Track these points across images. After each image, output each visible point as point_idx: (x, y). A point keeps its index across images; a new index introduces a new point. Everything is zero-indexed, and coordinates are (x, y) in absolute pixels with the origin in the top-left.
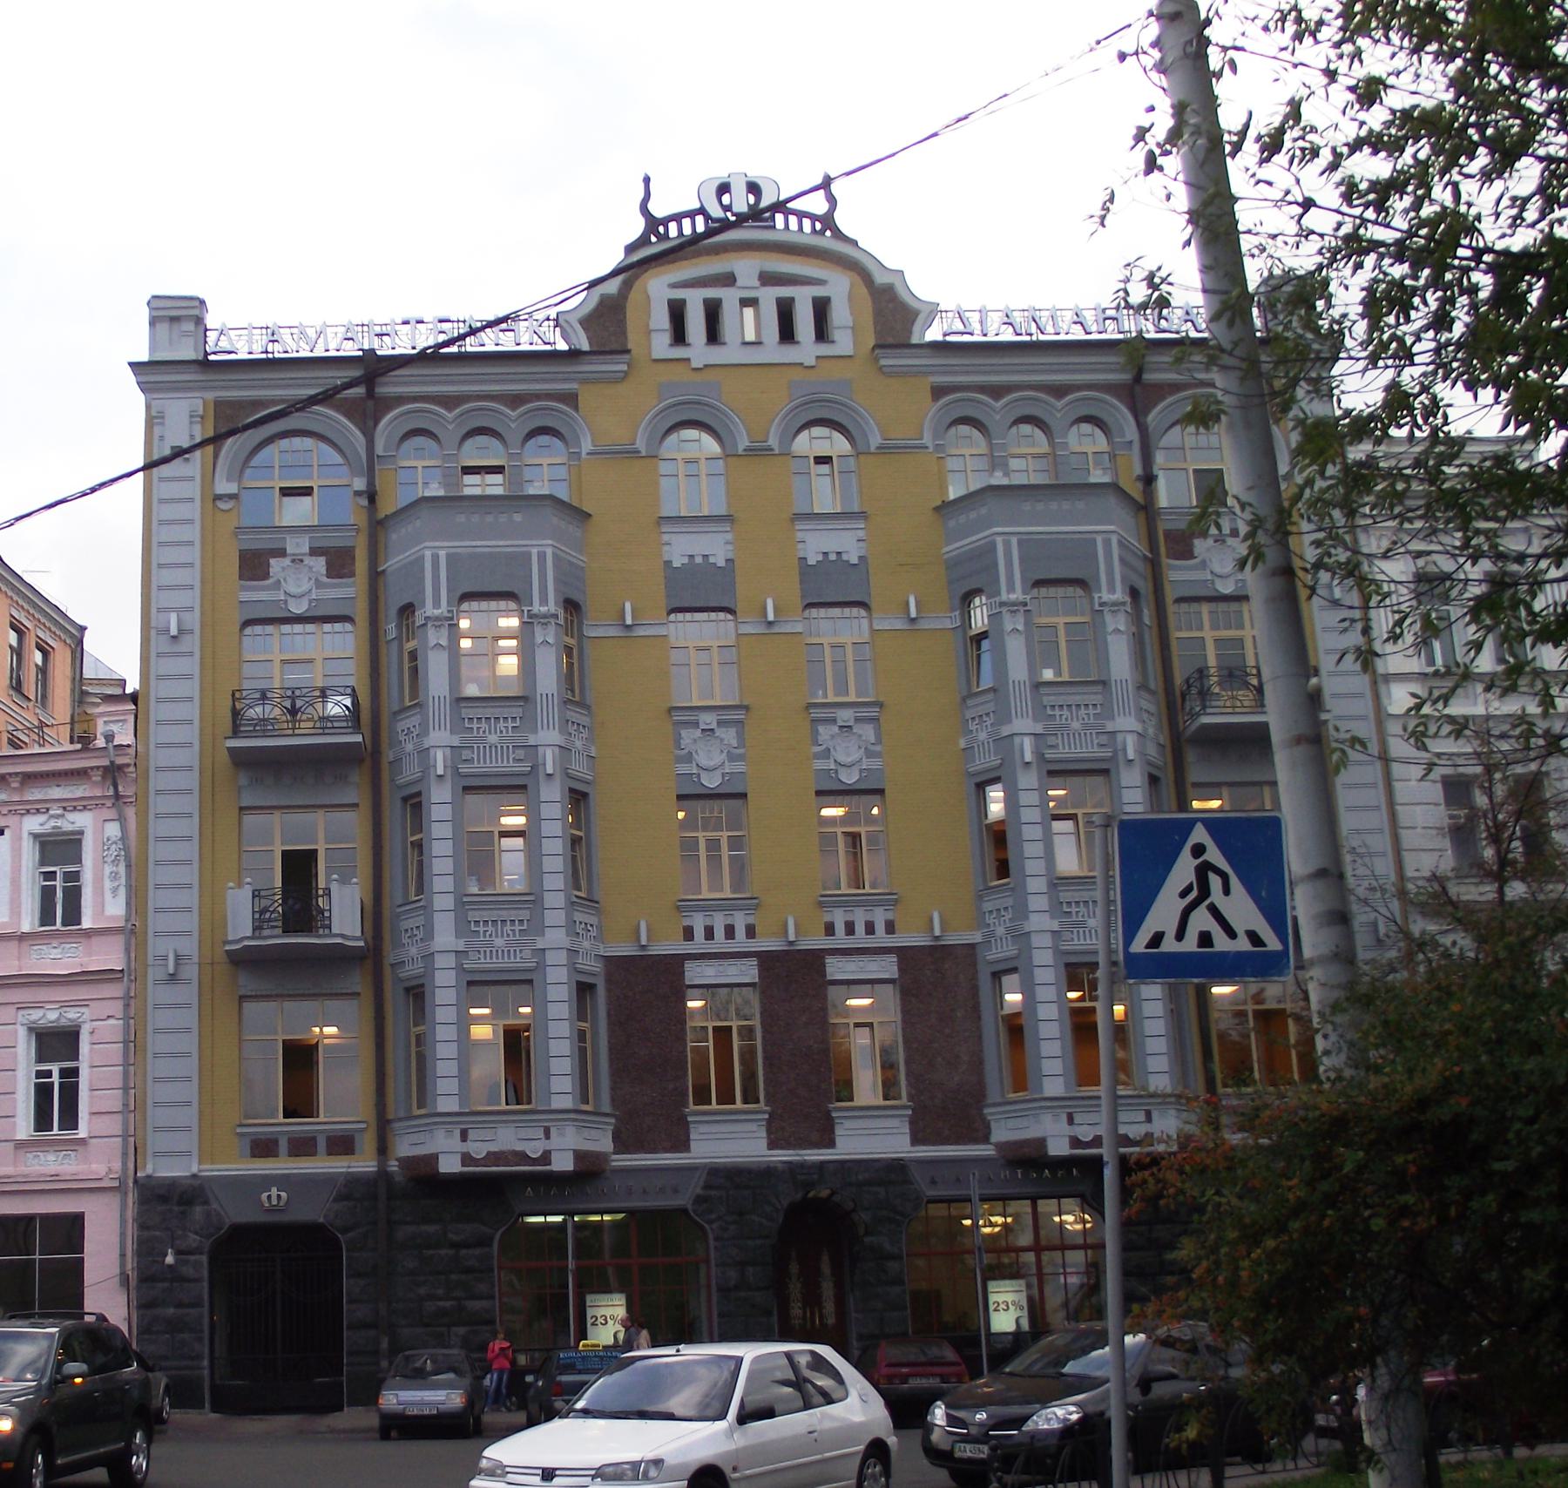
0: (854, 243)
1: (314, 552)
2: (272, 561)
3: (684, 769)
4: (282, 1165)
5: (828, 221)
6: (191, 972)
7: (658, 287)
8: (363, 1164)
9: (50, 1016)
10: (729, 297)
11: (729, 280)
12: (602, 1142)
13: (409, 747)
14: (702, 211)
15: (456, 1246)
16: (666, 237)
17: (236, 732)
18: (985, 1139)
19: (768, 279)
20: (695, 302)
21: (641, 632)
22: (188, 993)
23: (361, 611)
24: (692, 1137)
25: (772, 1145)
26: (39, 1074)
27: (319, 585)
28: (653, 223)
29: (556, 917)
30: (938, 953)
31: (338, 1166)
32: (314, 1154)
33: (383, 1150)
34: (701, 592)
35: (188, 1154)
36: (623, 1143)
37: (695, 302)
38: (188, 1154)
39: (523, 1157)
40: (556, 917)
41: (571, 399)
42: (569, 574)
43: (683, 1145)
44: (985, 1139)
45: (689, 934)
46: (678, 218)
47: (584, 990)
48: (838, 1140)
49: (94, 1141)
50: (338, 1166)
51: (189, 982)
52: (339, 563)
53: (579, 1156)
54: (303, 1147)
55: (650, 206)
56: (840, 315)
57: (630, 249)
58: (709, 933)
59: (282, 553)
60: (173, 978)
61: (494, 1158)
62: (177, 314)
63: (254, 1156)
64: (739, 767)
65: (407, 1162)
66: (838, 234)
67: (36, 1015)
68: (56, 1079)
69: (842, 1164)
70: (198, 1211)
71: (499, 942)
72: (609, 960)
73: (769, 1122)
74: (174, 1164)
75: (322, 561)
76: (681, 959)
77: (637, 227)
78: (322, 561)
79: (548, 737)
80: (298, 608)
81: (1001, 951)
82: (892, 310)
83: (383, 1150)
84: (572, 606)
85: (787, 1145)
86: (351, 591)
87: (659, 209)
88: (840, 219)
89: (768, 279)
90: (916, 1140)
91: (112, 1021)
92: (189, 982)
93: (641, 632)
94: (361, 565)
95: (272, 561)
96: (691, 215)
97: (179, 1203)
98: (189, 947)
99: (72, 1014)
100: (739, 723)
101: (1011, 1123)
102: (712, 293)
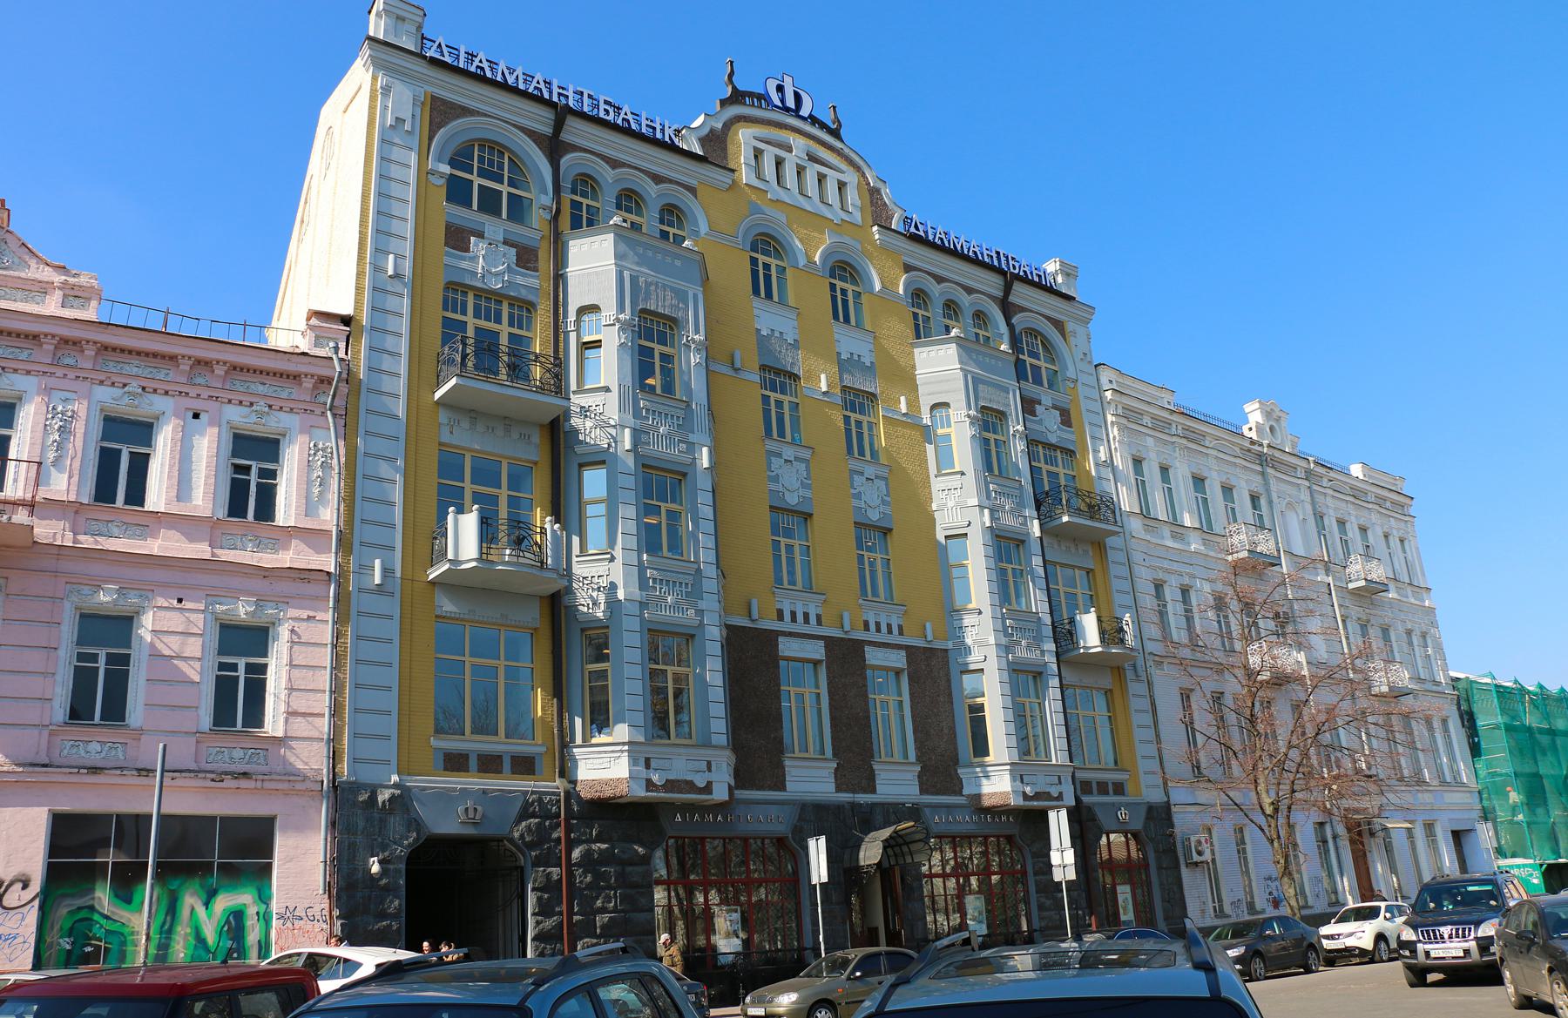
4: (473, 782)
25: (838, 789)
30: (930, 652)
32: (500, 772)
35: (388, 762)
37: (770, 153)
38: (388, 762)
39: (690, 786)
54: (490, 764)
61: (671, 785)
63: (446, 769)
69: (883, 804)
76: (776, 634)
85: (846, 791)
90: (923, 791)
92: (392, 594)
94: (545, 263)
96: (760, 97)
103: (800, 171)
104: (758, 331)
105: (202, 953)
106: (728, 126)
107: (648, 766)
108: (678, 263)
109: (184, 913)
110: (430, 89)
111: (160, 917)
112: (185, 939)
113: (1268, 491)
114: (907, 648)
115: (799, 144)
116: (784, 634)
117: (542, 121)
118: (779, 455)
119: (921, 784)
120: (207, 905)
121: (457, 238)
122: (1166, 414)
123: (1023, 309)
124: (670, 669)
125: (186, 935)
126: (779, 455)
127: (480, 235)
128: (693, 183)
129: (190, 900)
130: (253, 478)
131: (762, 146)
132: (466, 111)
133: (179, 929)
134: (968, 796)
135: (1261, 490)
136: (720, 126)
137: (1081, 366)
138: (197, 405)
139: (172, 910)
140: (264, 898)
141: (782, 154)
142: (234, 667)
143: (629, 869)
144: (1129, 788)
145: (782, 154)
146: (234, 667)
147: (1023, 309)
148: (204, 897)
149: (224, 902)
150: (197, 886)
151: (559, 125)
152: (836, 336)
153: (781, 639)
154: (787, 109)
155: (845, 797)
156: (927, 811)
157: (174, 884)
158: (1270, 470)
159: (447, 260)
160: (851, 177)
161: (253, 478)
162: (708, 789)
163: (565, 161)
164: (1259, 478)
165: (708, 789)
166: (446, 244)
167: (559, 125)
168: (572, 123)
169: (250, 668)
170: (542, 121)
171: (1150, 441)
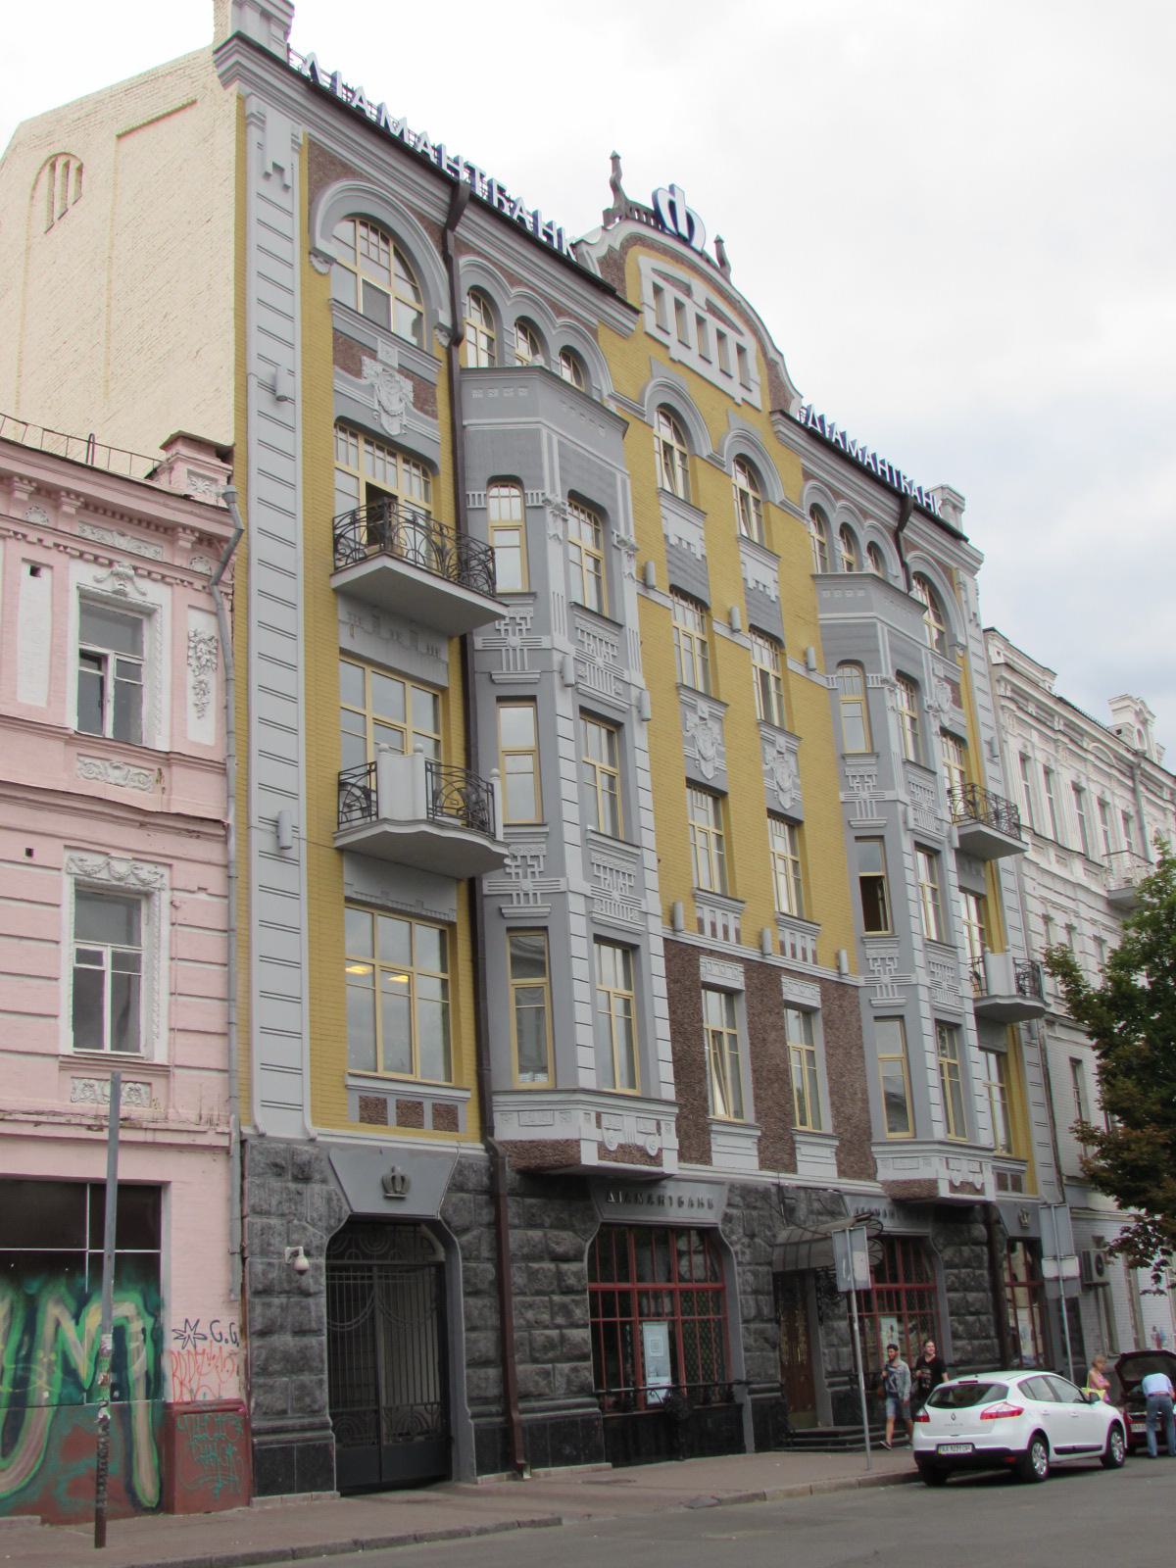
9: (119, 870)
15: (558, 1258)
18: (872, 1177)
22: (294, 878)
24: (714, 1148)
26: (82, 956)
32: (420, 1125)
33: (486, 1128)
44: (872, 1177)
48: (714, 1156)
49: (178, 1071)
51: (296, 862)
55: (624, 184)
63: (362, 1120)
67: (94, 861)
68: (107, 966)
70: (315, 1191)
73: (760, 1139)
81: (888, 998)
83: (486, 1128)
90: (842, 1173)
91: (202, 896)
92: (296, 862)
97: (296, 1179)
99: (146, 872)
101: (899, 1163)
103: (700, 321)
104: (666, 537)
105: (72, 1390)
107: (599, 1125)
109: (46, 1329)
111: (15, 1337)
112: (50, 1372)
113: (1139, 812)
114: (821, 980)
116: (711, 953)
119: (839, 1164)
120: (77, 1317)
122: (1050, 703)
123: (915, 547)
125: (51, 1364)
127: (373, 354)
129: (53, 1310)
130: (111, 672)
133: (40, 1354)
134: (884, 1183)
135: (1131, 811)
136: (617, 246)
137: (971, 629)
138: (39, 555)
139: (30, 1327)
140: (154, 1307)
141: (683, 298)
142: (96, 958)
143: (565, 1267)
144: (1026, 1182)
145: (683, 298)
146: (96, 958)
147: (915, 547)
148: (72, 1303)
149: (93, 1316)
150: (63, 1289)
152: (743, 557)
153: (703, 959)
154: (679, 237)
156: (847, 1199)
157: (33, 1287)
158: (1141, 788)
161: (111, 672)
164: (1128, 796)
166: (335, 362)
169: (119, 960)
170: (432, 201)
171: (1035, 737)
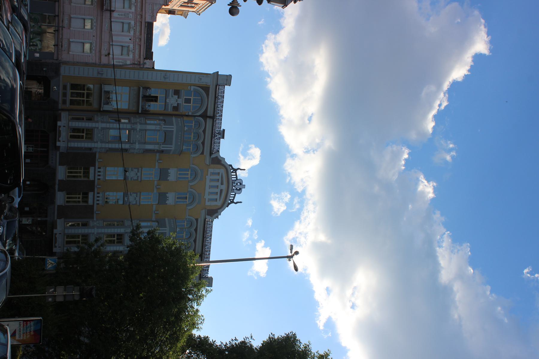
0: (227, 206)
1: (178, 104)
2: (177, 96)
3: (130, 169)
5: (232, 202)
6: (99, 76)
7: (222, 171)
8: (60, 106)
10: (219, 184)
11: (222, 184)
12: (61, 151)
13: (138, 120)
14: (237, 179)
16: (232, 172)
17: (143, 88)
19: (221, 191)
20: (219, 177)
21: (157, 163)
23: (166, 112)
27: (172, 104)
28: (235, 170)
29: (104, 145)
31: (60, 101)
34: (163, 174)
36: (61, 154)
40: (104, 145)
41: (202, 153)
42: (168, 152)
43: (60, 164)
45: (99, 168)
46: (236, 175)
47: (90, 149)
50: (60, 101)
52: (176, 108)
53: (59, 147)
56: (214, 203)
57: (231, 166)
58: (99, 172)
59: (178, 98)
60: (98, 73)
62: (228, 80)
64: (130, 179)
65: (60, 114)
66: (229, 204)
71: (99, 135)
72: (95, 154)
74: (64, 71)
75: (176, 105)
77: (235, 167)
78: (176, 105)
79: (137, 146)
80: (168, 100)
82: (215, 213)
84: (162, 151)
86: (170, 110)
87: (238, 172)
88: (232, 205)
89: (221, 191)
93: (157, 163)
95: (177, 96)
96: (237, 177)
98: (104, 76)
100: (137, 180)
102: (220, 180)
106: (223, 165)
108: (179, 143)
110: (211, 87)
115: (224, 187)
117: (210, 113)
118: (138, 172)
121: (177, 93)
124: (84, 134)
126: (138, 172)
128: (205, 154)
131: (220, 174)
132: (208, 95)
151: (210, 117)
155: (57, 182)
159: (171, 90)
160: (219, 203)
162: (59, 141)
163: (201, 119)
165: (59, 141)
167: (210, 117)
168: (211, 120)
